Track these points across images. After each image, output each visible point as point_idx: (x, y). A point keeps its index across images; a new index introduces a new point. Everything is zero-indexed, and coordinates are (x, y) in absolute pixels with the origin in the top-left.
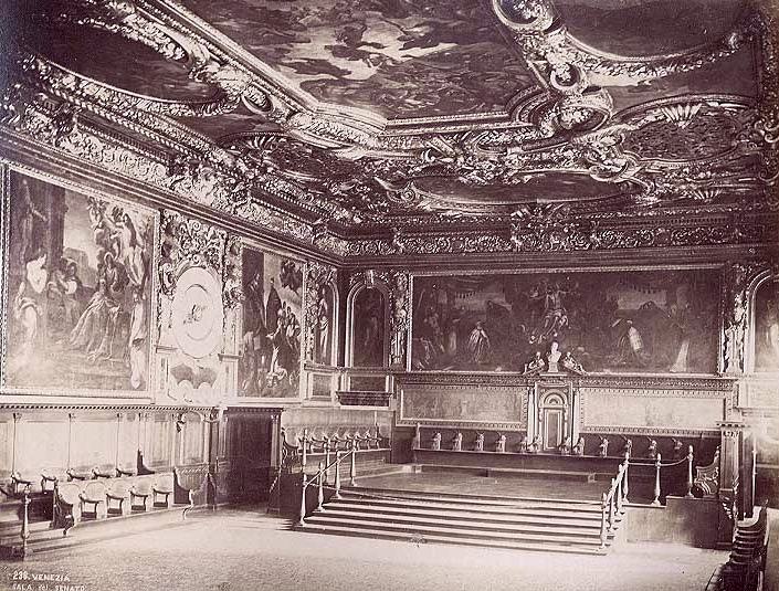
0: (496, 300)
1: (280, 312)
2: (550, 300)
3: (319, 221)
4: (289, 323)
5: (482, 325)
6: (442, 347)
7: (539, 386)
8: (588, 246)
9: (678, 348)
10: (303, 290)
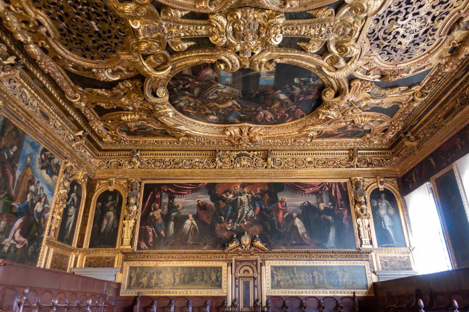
0: (202, 200)
1: (32, 188)
2: (241, 200)
3: (80, 133)
4: (40, 200)
5: (194, 216)
6: (162, 233)
7: (236, 261)
8: (265, 165)
9: (329, 232)
10: (60, 178)
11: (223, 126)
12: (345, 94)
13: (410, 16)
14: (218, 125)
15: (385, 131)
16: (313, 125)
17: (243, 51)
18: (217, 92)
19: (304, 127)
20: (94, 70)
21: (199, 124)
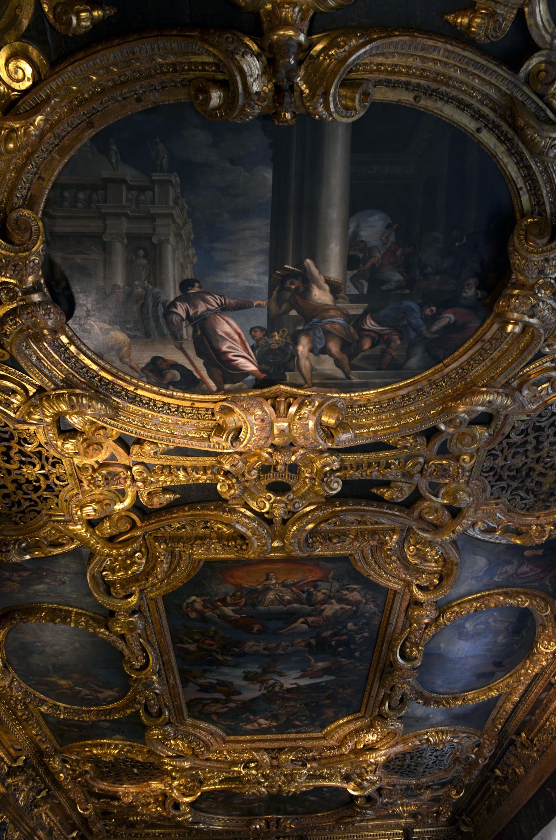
11: (247, 818)
12: (376, 801)
13: (415, 758)
14: (241, 818)
15: (438, 812)
16: (350, 817)
17: (271, 787)
18: (243, 799)
19: (342, 817)
20: (121, 793)
21: (218, 819)
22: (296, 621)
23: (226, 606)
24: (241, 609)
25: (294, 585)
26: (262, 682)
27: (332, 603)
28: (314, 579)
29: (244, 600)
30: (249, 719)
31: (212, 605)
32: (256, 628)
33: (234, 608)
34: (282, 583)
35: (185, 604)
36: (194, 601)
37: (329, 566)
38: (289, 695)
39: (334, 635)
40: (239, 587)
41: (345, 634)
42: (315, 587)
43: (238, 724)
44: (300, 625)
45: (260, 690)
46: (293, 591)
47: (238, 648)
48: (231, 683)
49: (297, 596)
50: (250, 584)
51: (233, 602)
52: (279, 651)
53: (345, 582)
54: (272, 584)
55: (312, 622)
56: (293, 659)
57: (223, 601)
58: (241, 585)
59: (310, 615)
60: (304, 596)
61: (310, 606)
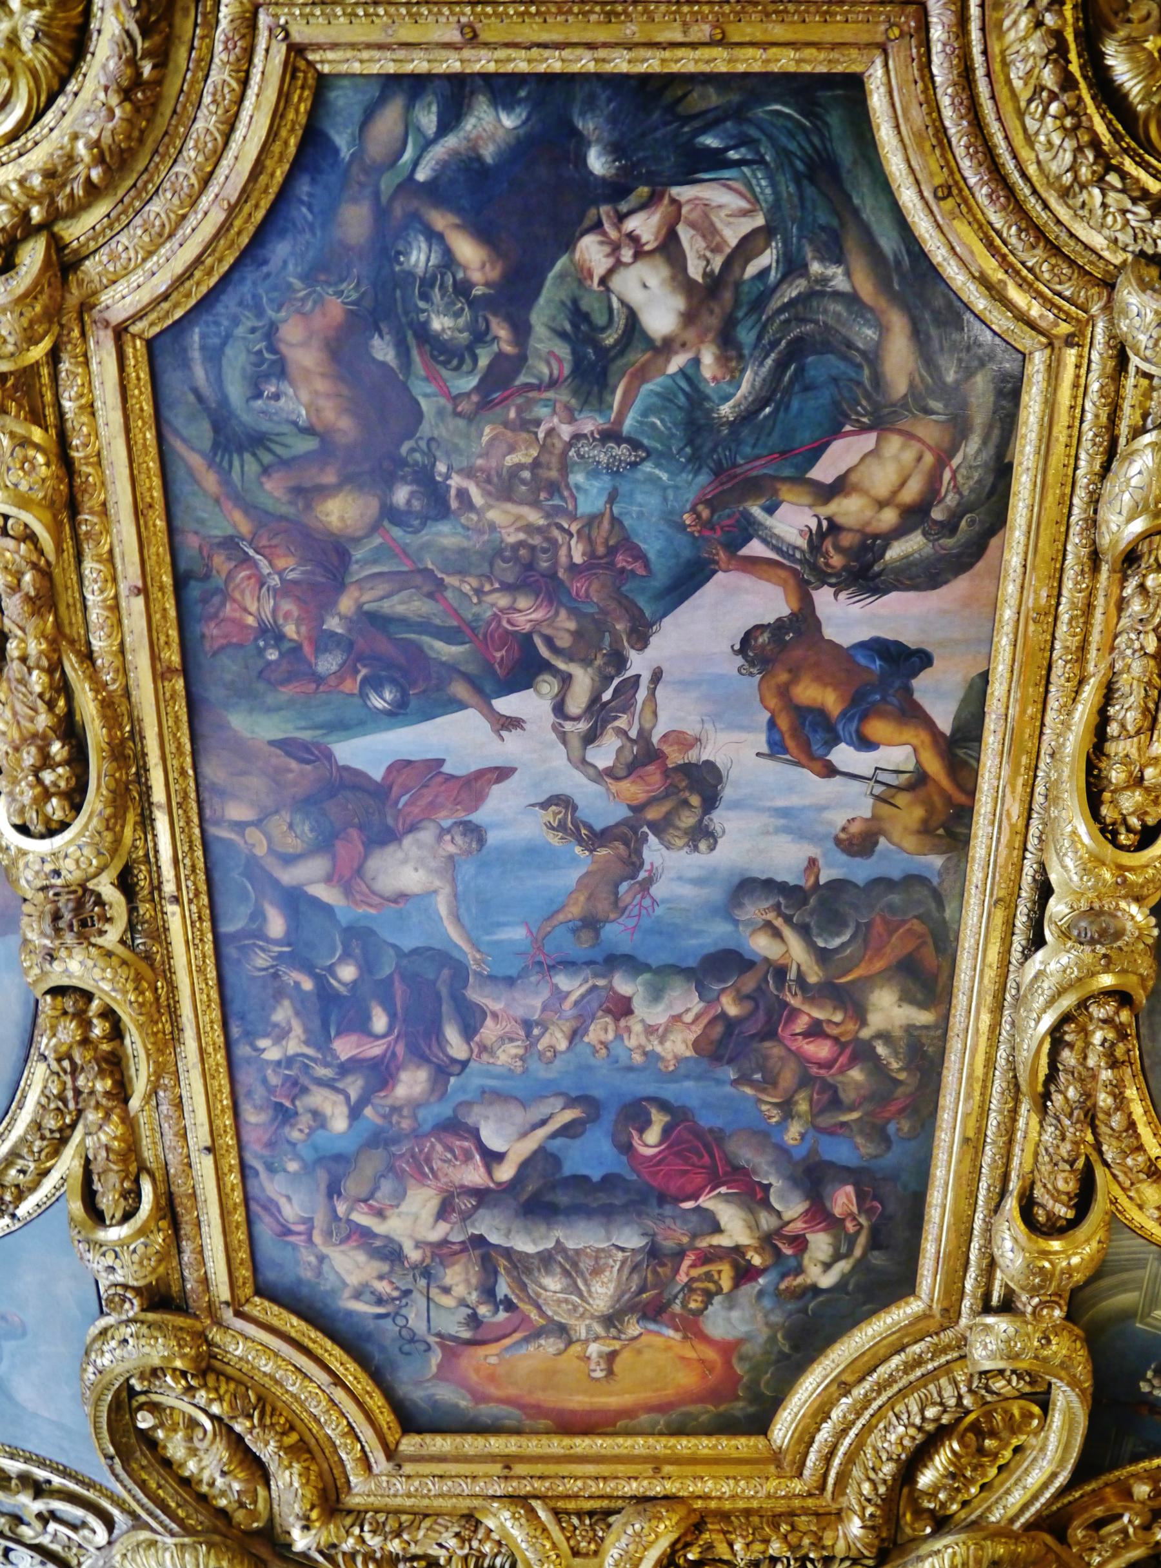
22: (525, 1166)
23: (738, 1250)
24: (694, 1236)
25: (537, 1334)
26: (644, 755)
27: (418, 1245)
28: (481, 1351)
29: (682, 1278)
30: (726, 340)
31: (778, 1253)
32: (653, 1135)
33: (717, 1240)
34: (570, 1342)
35: (858, 1252)
36: (827, 1266)
37: (447, 1394)
38: (527, 613)
39: (381, 1074)
40: (691, 1327)
41: (345, 1069)
42: (474, 1320)
43: (793, 266)
44: (509, 1137)
45: (657, 676)
46: (539, 1307)
47: (723, 1015)
48: (776, 749)
49: (524, 1287)
50: (658, 1341)
51: (713, 1268)
52: (572, 985)
53: (387, 1324)
54: (597, 1338)
55: (468, 1157)
56: (518, 934)
57: (745, 1274)
58: (685, 1338)
59: (481, 1196)
60: (503, 1288)
61: (479, 1241)
